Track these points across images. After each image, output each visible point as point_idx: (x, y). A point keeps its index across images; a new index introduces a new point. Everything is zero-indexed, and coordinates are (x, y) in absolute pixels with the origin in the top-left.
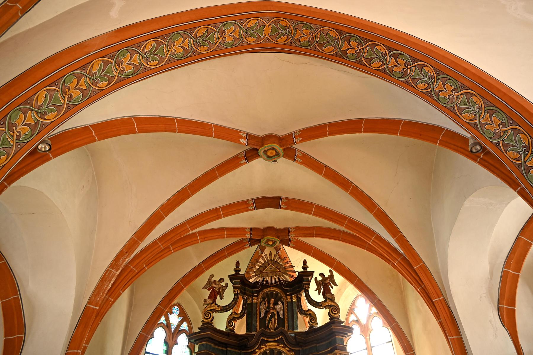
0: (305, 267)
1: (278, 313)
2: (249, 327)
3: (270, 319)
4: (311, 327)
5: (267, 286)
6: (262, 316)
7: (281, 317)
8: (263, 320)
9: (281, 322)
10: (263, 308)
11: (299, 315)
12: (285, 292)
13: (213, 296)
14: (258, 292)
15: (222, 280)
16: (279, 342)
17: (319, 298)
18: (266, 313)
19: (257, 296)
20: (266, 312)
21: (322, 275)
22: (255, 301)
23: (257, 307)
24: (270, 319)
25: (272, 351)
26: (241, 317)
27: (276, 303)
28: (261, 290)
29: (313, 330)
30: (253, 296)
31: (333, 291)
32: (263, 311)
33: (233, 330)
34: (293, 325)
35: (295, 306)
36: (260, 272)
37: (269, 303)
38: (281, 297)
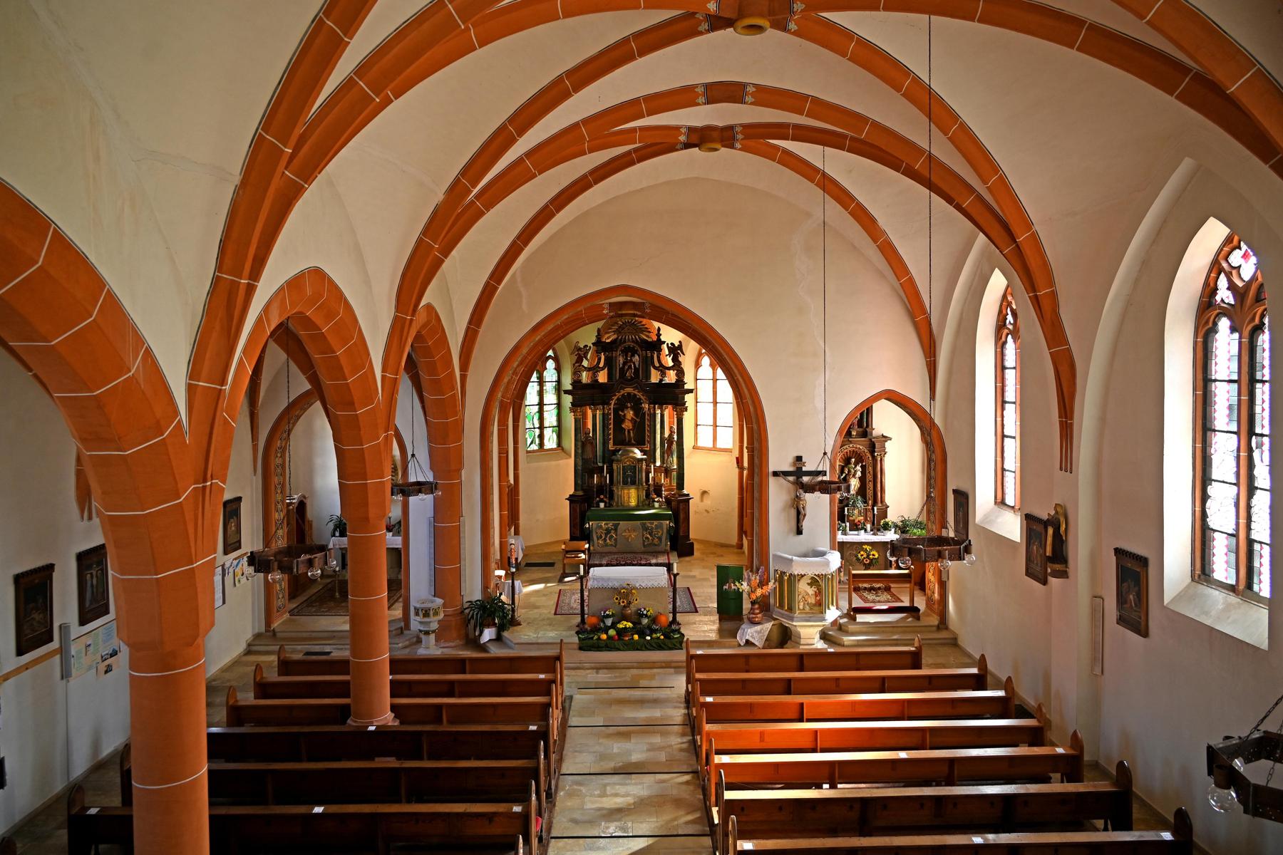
0: (659, 335)
1: (634, 363)
2: (610, 376)
3: (628, 370)
4: (661, 380)
5: (625, 342)
6: (621, 366)
7: (637, 366)
8: (622, 370)
9: (637, 370)
10: (621, 360)
11: (652, 368)
12: (641, 347)
13: (580, 360)
14: (617, 348)
15: (586, 346)
16: (635, 388)
17: (669, 362)
18: (625, 364)
19: (616, 351)
20: (624, 362)
21: (672, 344)
22: (614, 355)
23: (616, 360)
24: (628, 370)
25: (629, 394)
26: (602, 369)
27: (633, 355)
28: (620, 345)
29: (660, 385)
30: (612, 351)
31: (680, 359)
32: (621, 362)
33: (597, 381)
34: (648, 376)
35: (649, 359)
36: (618, 331)
37: (627, 356)
38: (637, 350)
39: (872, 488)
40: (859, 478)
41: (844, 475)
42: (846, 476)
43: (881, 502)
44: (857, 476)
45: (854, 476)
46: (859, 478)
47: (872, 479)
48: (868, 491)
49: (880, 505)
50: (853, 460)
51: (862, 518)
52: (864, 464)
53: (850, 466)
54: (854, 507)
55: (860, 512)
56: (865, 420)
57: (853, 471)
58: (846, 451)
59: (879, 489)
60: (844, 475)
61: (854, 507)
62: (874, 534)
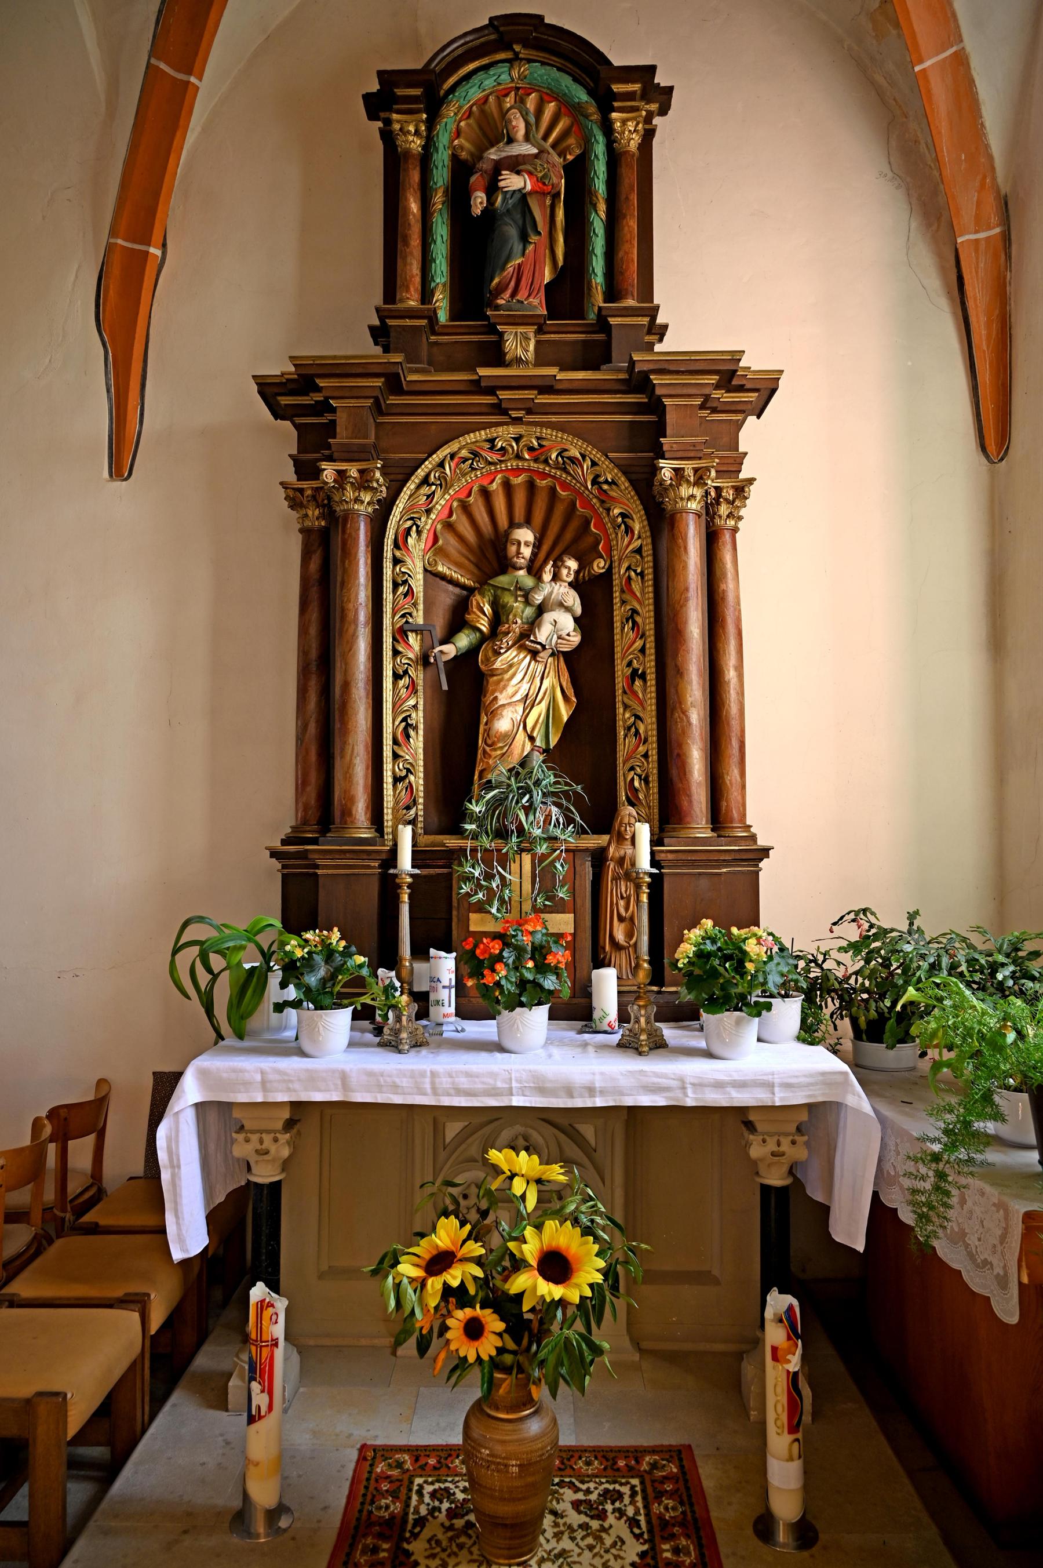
39: (648, 726)
40: (571, 659)
41: (464, 640)
42: (472, 652)
43: (718, 818)
44: (543, 634)
45: (525, 640)
46: (571, 659)
47: (650, 665)
48: (625, 745)
49: (700, 827)
50: (525, 535)
51: (563, 923)
52: (599, 566)
53: (503, 580)
54: (502, 834)
55: (543, 877)
56: (598, 265)
57: (520, 612)
58: (473, 479)
59: (696, 716)
60: (464, 640)
61: (502, 834)
62: (628, 1046)
